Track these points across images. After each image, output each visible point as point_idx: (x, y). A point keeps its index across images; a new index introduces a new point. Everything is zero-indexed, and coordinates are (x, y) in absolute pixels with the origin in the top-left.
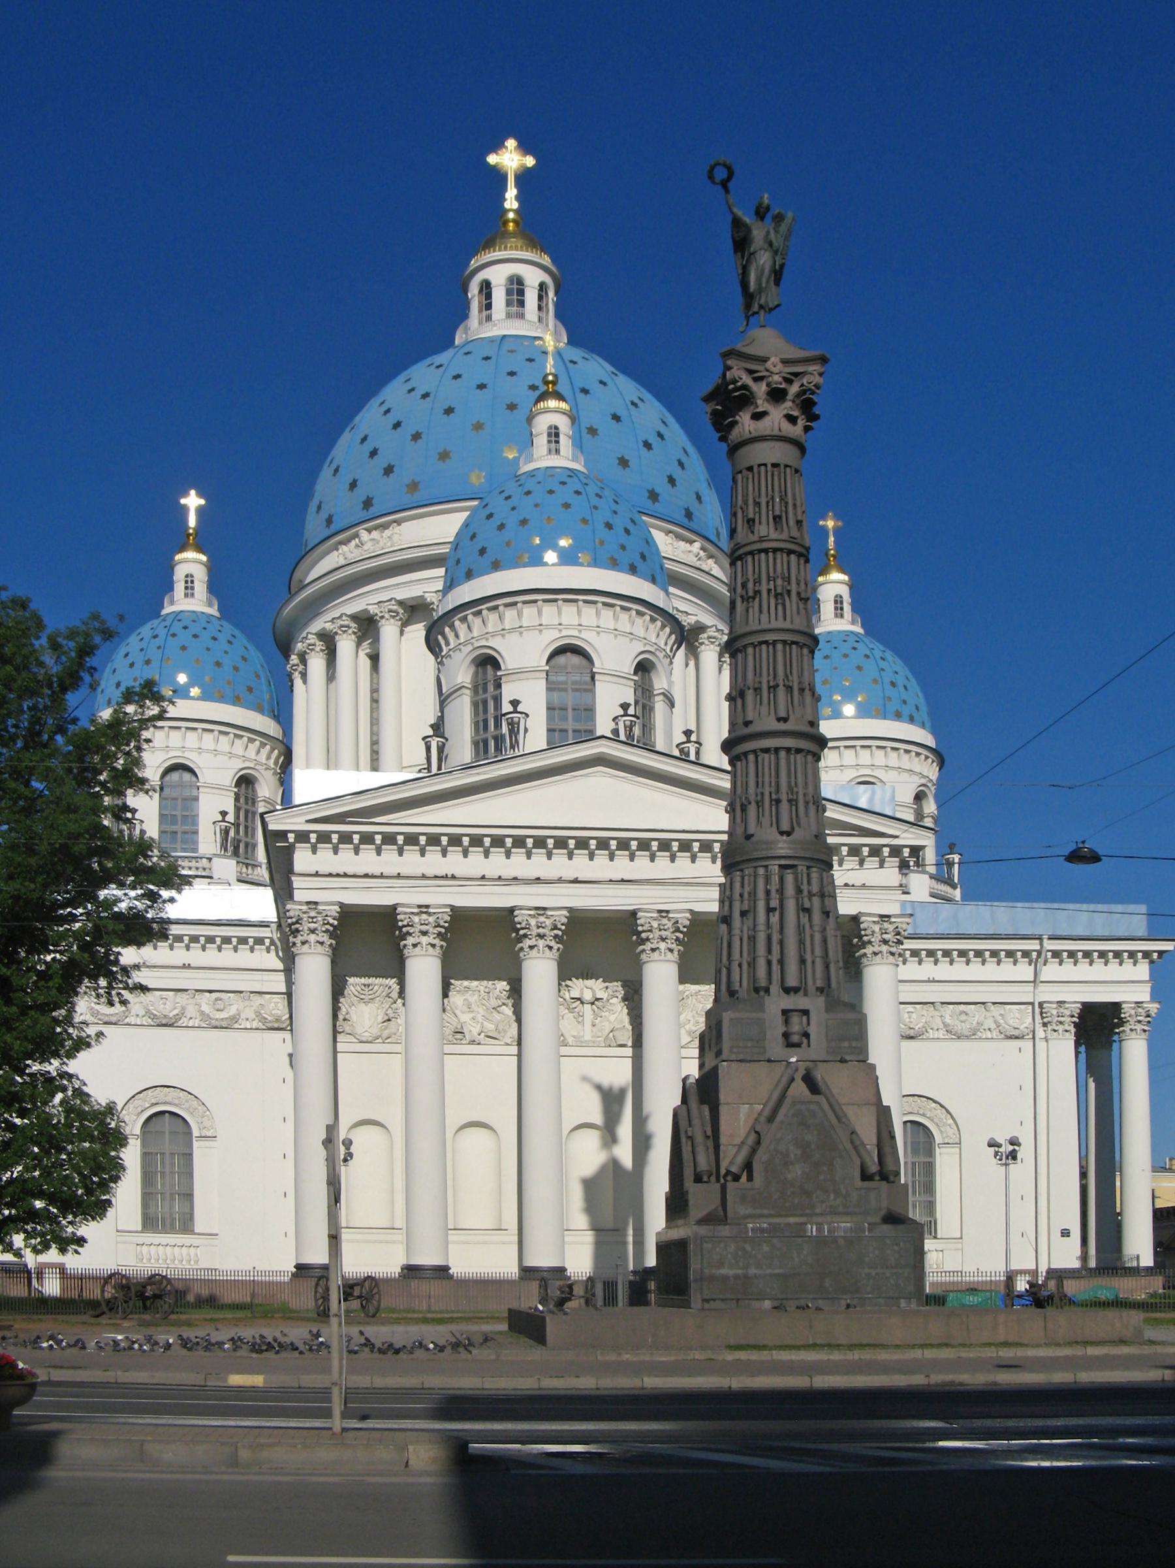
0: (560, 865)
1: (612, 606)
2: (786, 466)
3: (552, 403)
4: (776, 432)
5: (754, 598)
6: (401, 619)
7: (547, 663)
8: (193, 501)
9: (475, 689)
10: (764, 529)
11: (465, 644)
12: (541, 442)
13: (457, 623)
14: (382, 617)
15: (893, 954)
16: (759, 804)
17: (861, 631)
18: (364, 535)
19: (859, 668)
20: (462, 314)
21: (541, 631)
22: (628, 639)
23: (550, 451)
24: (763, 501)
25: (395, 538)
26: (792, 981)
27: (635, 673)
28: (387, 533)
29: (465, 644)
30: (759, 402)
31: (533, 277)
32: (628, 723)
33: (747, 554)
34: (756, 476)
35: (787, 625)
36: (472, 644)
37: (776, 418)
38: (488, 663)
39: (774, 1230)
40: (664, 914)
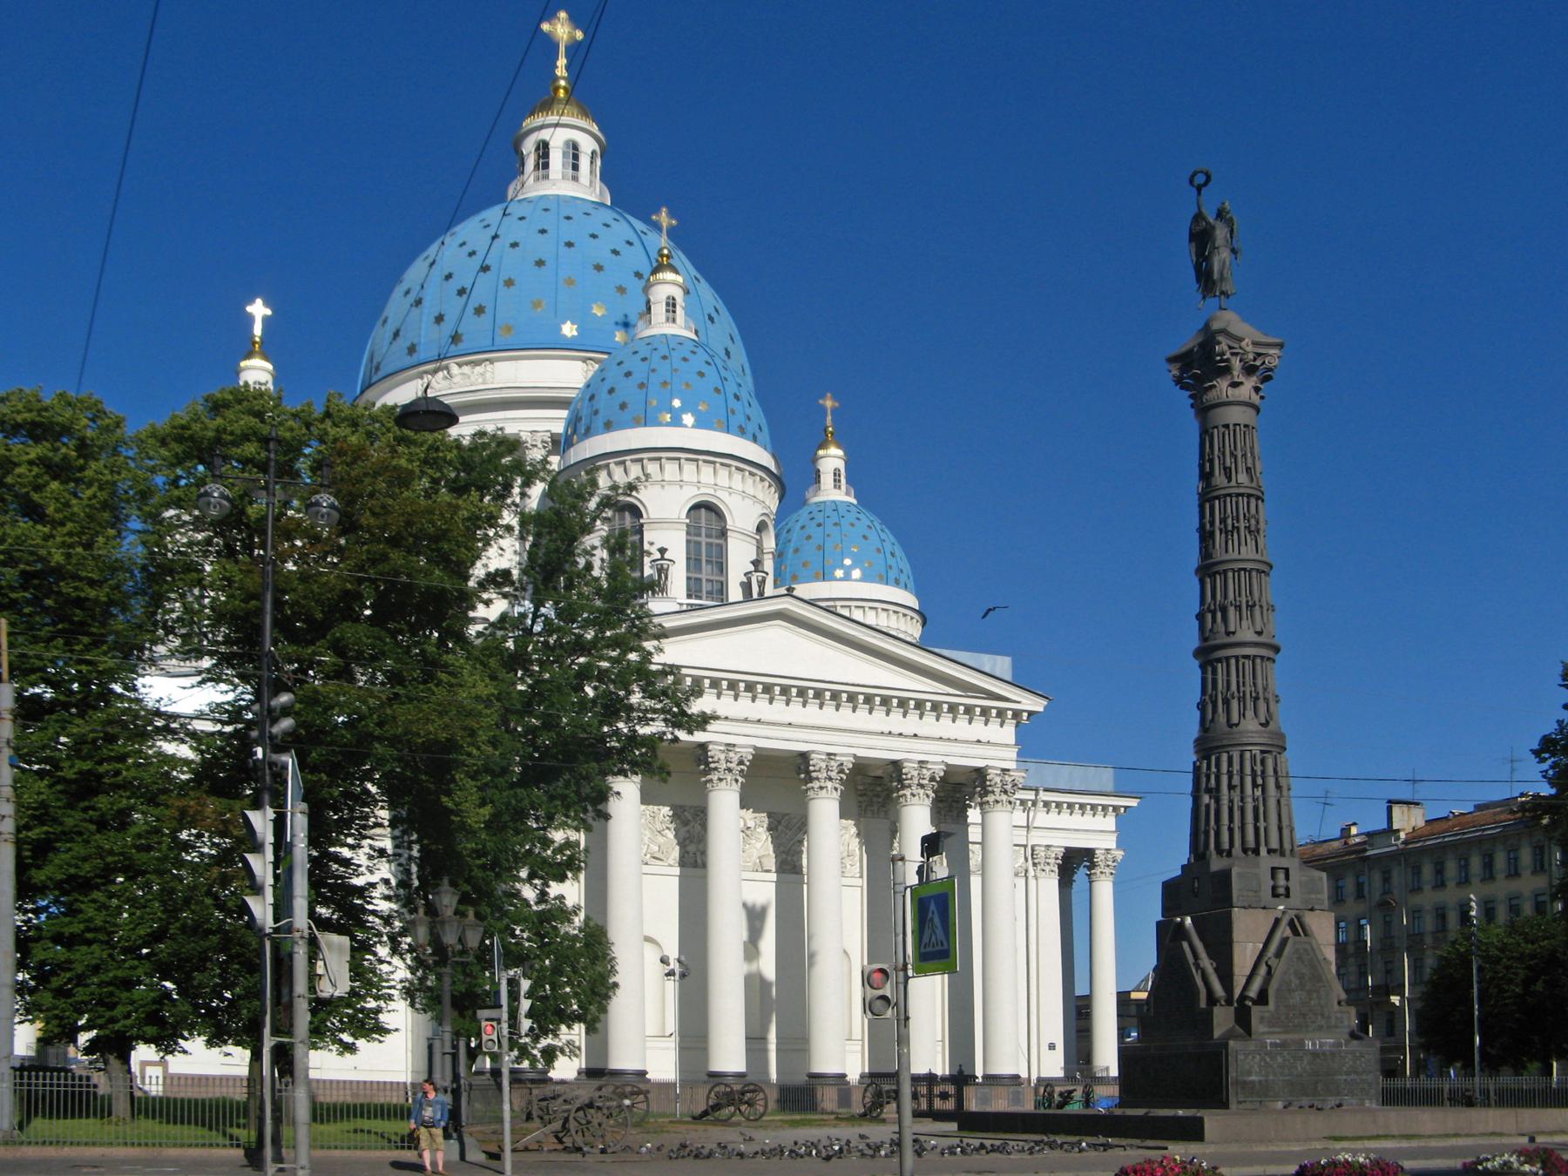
3: (669, 276)
7: (688, 516)
8: (258, 310)
10: (1243, 478)
12: (659, 311)
16: (1242, 699)
18: (455, 369)
19: (865, 537)
23: (667, 320)
24: (1239, 455)
25: (488, 375)
26: (1274, 844)
28: (478, 369)
30: (1235, 373)
35: (1258, 557)
39: (1283, 1045)
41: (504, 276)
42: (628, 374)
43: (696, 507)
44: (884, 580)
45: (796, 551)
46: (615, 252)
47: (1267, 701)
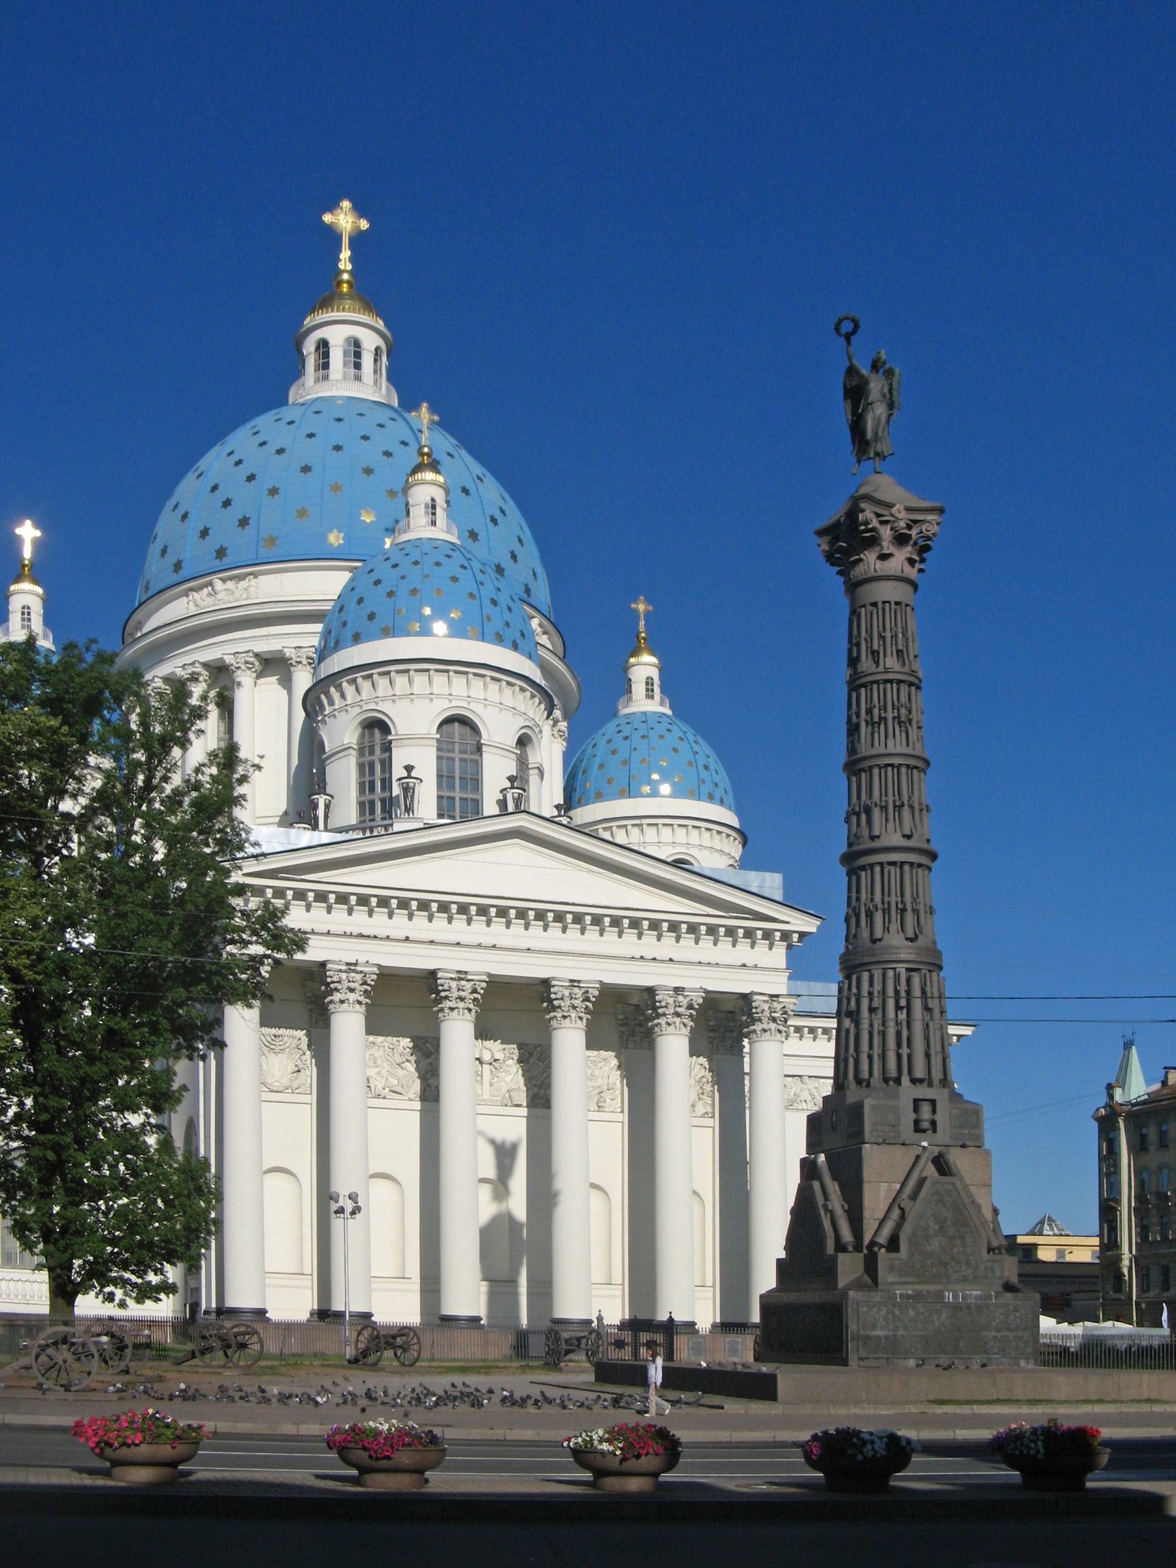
0: (478, 931)
1: (499, 680)
2: (907, 605)
3: (429, 476)
4: (899, 573)
5: (879, 724)
6: (256, 671)
7: (438, 732)
8: (28, 532)
9: (361, 751)
10: (891, 662)
11: (353, 705)
13: (345, 685)
14: (239, 668)
15: (780, 1032)
16: (886, 911)
17: (669, 712)
18: (219, 585)
19: (675, 750)
20: (297, 371)
21: (431, 700)
22: (511, 713)
24: (888, 635)
25: (252, 590)
26: (919, 1073)
28: (243, 584)
29: (353, 705)
30: (885, 544)
31: (370, 341)
32: (516, 795)
33: (872, 682)
34: (880, 612)
35: (909, 751)
36: (361, 707)
37: (899, 561)
38: (376, 727)
39: (918, 1297)
40: (576, 984)
41: (269, 485)
42: (378, 582)
43: (449, 721)
44: (696, 795)
45: (601, 766)
46: (388, 454)
47: (916, 912)
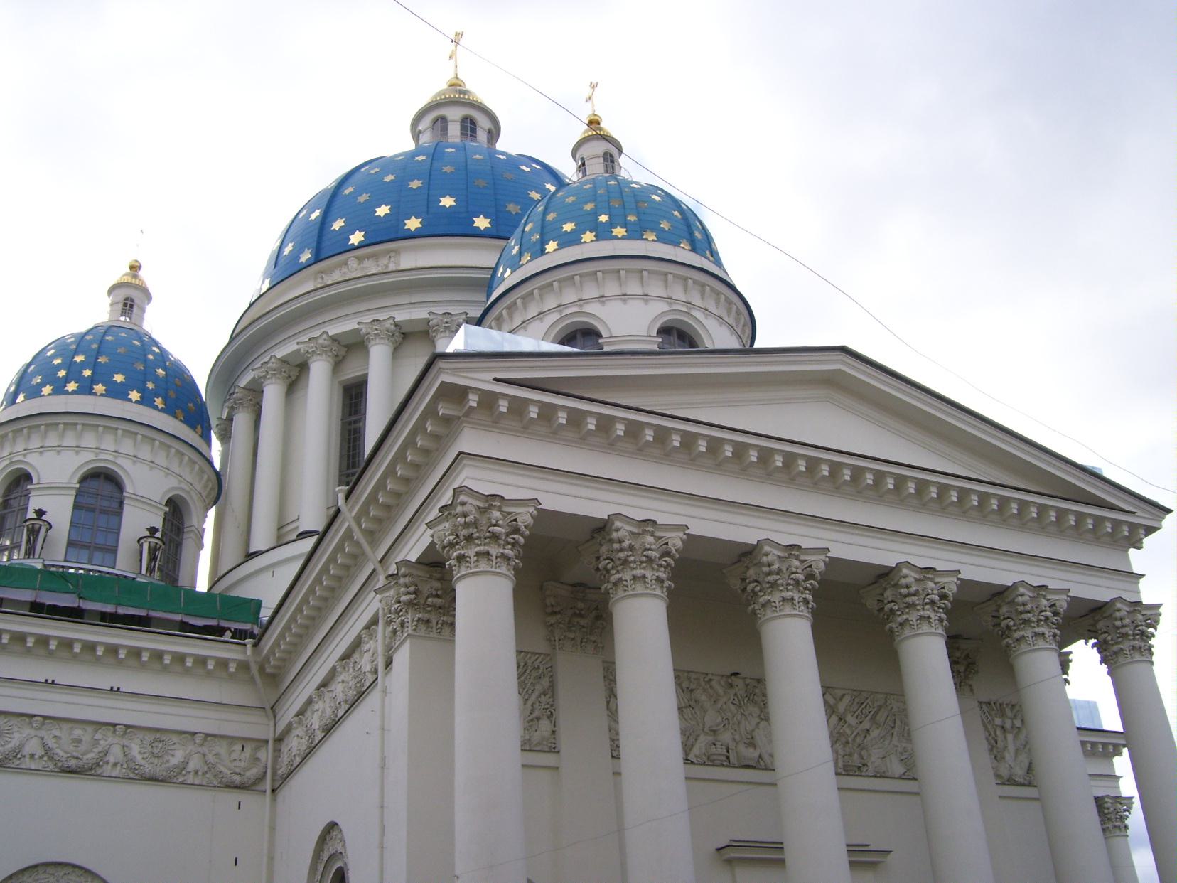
27: (167, 504)
32: (153, 545)
